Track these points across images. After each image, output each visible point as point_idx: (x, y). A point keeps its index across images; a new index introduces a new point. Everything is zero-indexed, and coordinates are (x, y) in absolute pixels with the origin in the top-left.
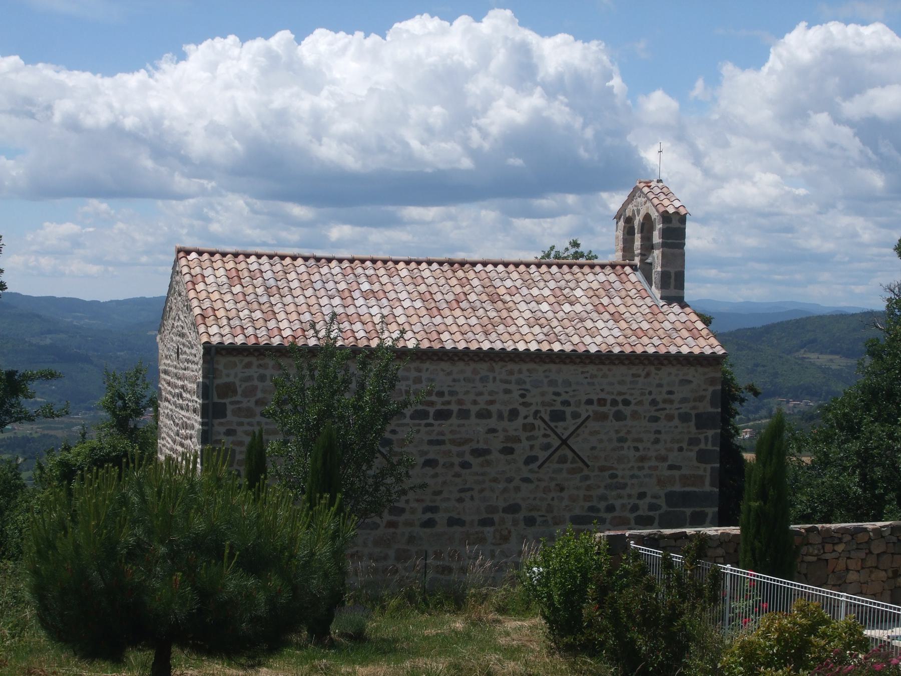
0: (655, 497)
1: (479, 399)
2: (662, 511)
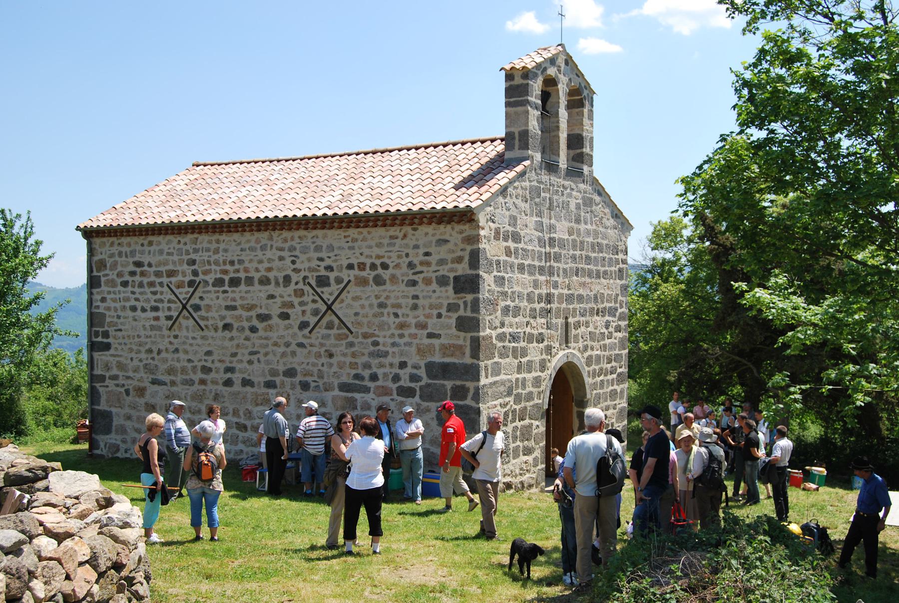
0: (416, 367)
1: (260, 266)
2: (423, 383)
